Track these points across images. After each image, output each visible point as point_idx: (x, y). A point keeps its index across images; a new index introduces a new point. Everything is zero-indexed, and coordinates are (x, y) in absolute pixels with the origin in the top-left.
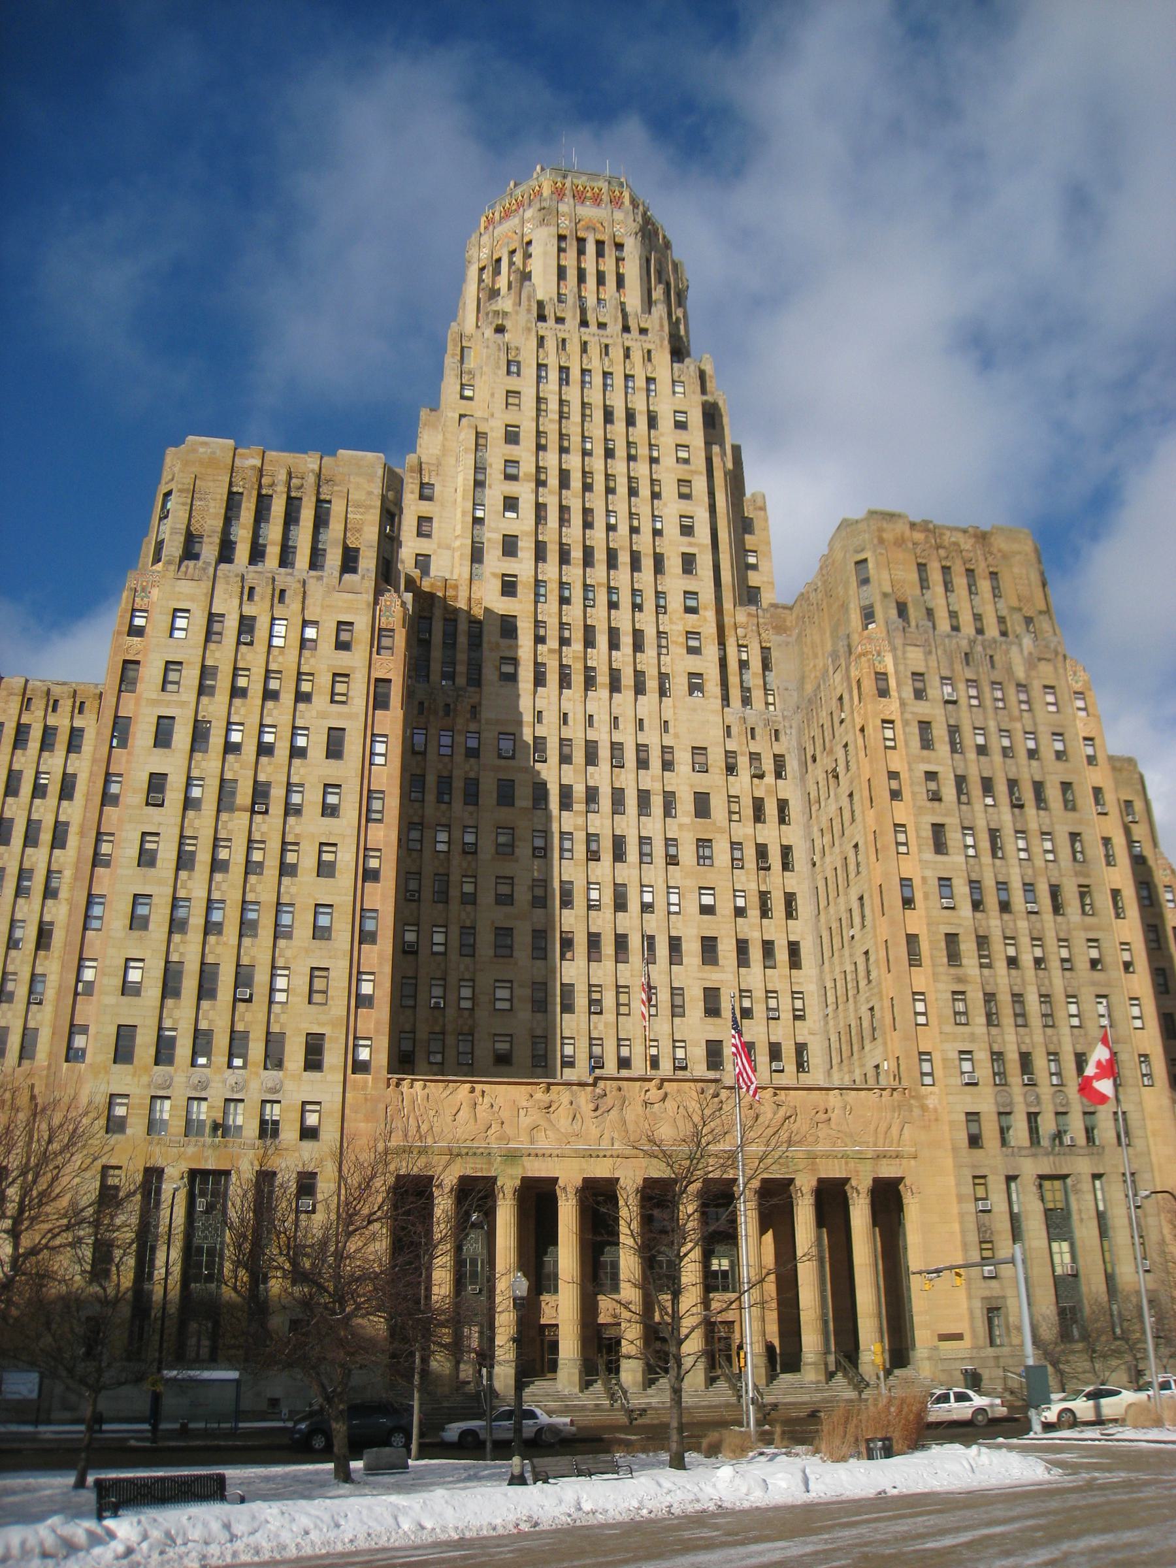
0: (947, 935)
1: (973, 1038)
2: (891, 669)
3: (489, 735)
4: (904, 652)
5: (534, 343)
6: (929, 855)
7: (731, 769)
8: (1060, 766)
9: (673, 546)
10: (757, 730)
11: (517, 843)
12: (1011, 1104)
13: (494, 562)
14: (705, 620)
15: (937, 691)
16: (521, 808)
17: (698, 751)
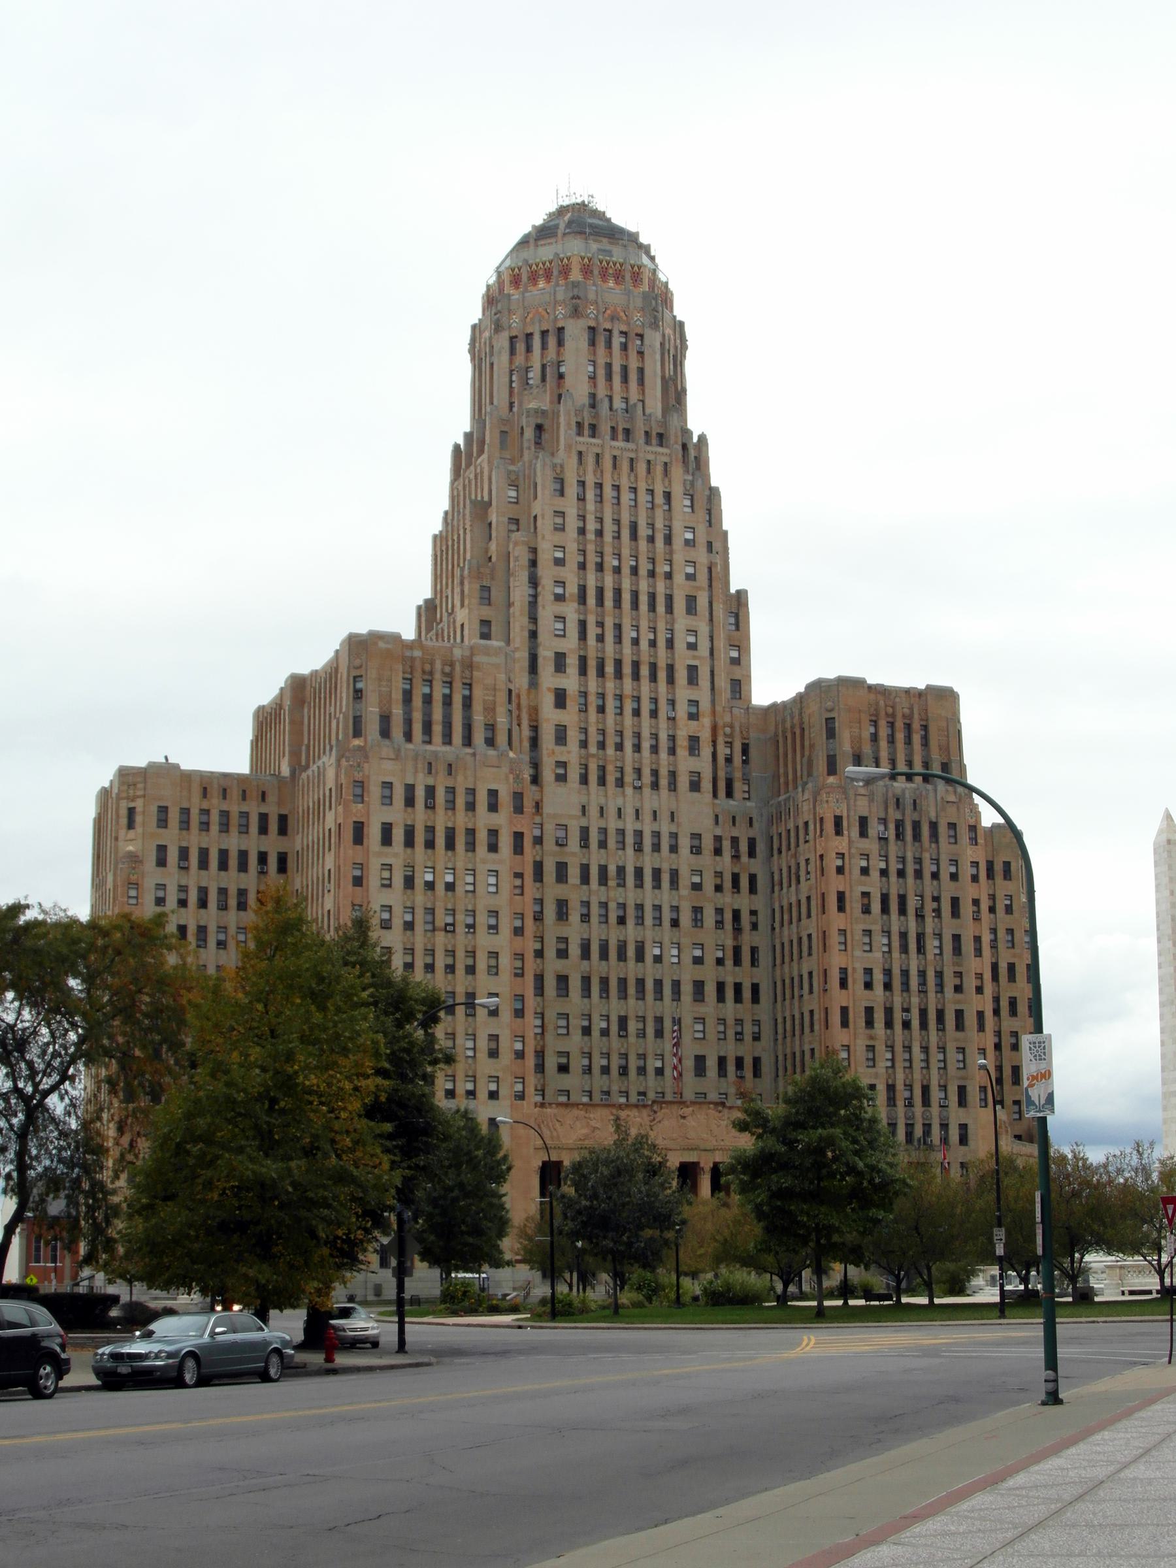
0: (866, 1008)
1: (876, 1076)
2: (845, 815)
3: (549, 828)
4: (855, 800)
5: (574, 460)
6: (858, 953)
7: (718, 852)
8: (953, 884)
9: (683, 658)
10: (737, 818)
11: (570, 912)
12: (896, 1118)
13: (549, 679)
14: (703, 726)
15: (875, 829)
16: (574, 885)
17: (696, 836)
